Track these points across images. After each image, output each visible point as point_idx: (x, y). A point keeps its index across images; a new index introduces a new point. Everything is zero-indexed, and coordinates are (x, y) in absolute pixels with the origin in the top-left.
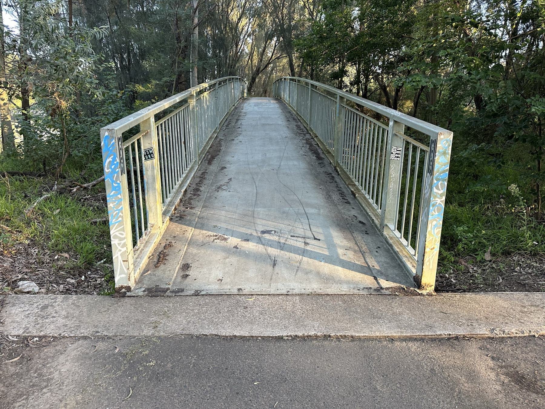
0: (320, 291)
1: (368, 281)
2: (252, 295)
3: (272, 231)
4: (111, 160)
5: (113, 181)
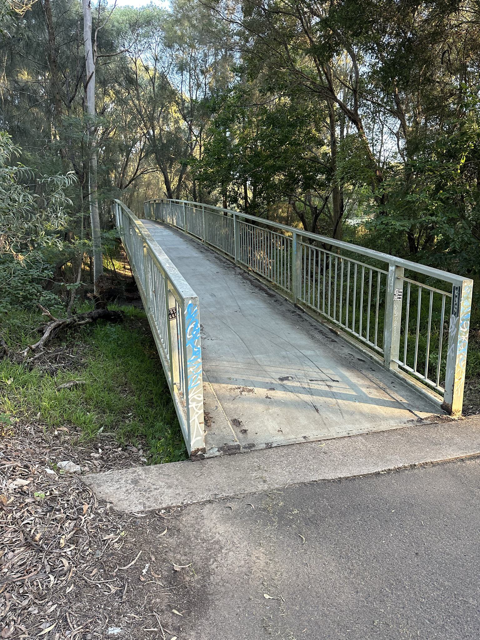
0: (375, 429)
1: (406, 414)
2: (320, 441)
3: (288, 377)
4: (193, 326)
5: (194, 346)
